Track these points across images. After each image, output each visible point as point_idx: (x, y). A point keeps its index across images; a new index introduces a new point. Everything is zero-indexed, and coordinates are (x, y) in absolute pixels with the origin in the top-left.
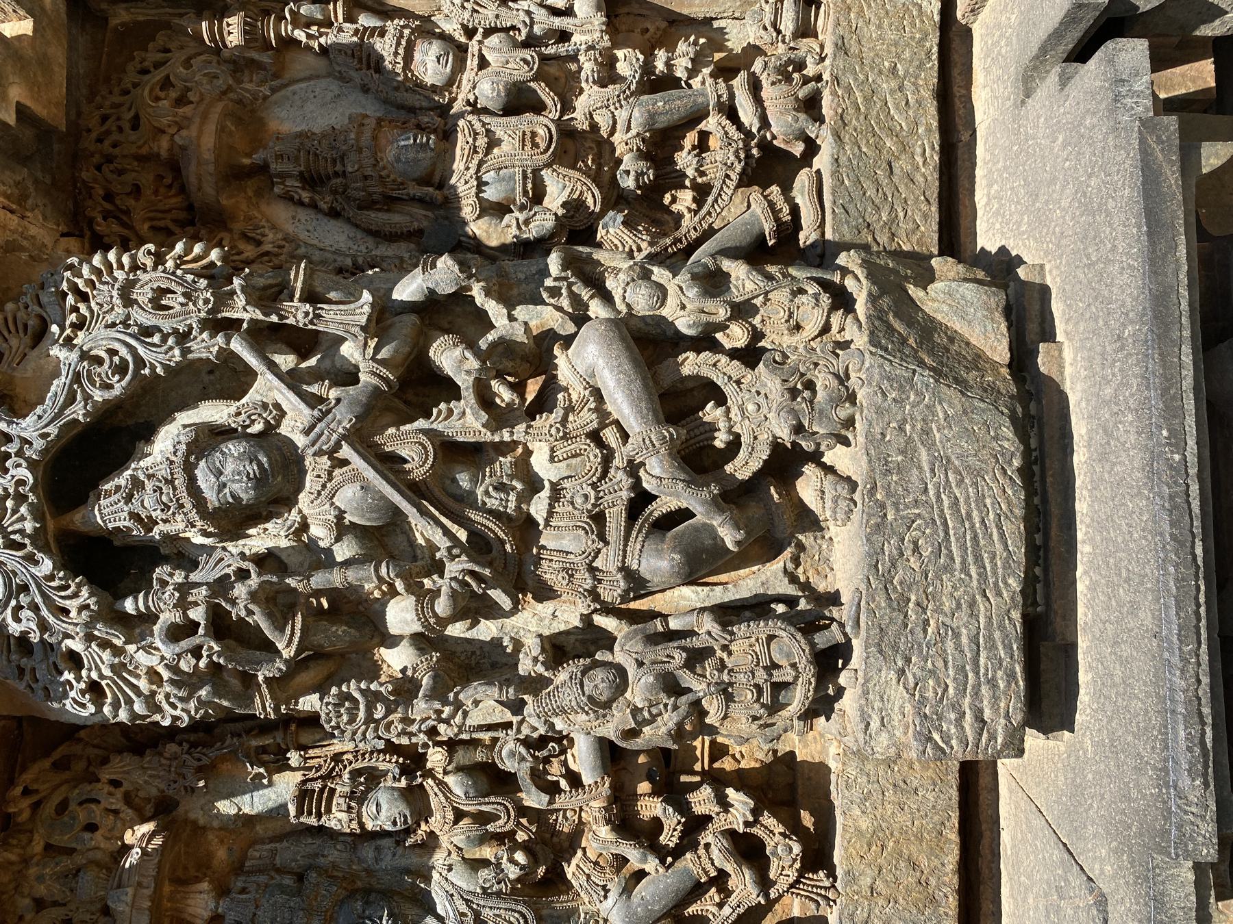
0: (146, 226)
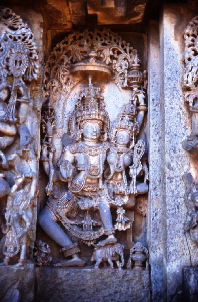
0: (71, 49)
